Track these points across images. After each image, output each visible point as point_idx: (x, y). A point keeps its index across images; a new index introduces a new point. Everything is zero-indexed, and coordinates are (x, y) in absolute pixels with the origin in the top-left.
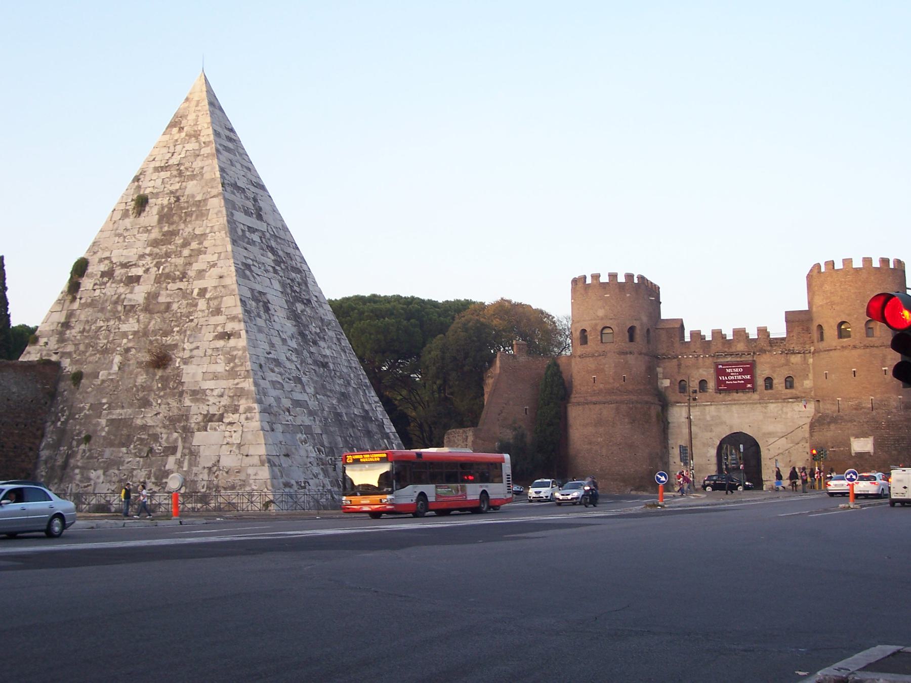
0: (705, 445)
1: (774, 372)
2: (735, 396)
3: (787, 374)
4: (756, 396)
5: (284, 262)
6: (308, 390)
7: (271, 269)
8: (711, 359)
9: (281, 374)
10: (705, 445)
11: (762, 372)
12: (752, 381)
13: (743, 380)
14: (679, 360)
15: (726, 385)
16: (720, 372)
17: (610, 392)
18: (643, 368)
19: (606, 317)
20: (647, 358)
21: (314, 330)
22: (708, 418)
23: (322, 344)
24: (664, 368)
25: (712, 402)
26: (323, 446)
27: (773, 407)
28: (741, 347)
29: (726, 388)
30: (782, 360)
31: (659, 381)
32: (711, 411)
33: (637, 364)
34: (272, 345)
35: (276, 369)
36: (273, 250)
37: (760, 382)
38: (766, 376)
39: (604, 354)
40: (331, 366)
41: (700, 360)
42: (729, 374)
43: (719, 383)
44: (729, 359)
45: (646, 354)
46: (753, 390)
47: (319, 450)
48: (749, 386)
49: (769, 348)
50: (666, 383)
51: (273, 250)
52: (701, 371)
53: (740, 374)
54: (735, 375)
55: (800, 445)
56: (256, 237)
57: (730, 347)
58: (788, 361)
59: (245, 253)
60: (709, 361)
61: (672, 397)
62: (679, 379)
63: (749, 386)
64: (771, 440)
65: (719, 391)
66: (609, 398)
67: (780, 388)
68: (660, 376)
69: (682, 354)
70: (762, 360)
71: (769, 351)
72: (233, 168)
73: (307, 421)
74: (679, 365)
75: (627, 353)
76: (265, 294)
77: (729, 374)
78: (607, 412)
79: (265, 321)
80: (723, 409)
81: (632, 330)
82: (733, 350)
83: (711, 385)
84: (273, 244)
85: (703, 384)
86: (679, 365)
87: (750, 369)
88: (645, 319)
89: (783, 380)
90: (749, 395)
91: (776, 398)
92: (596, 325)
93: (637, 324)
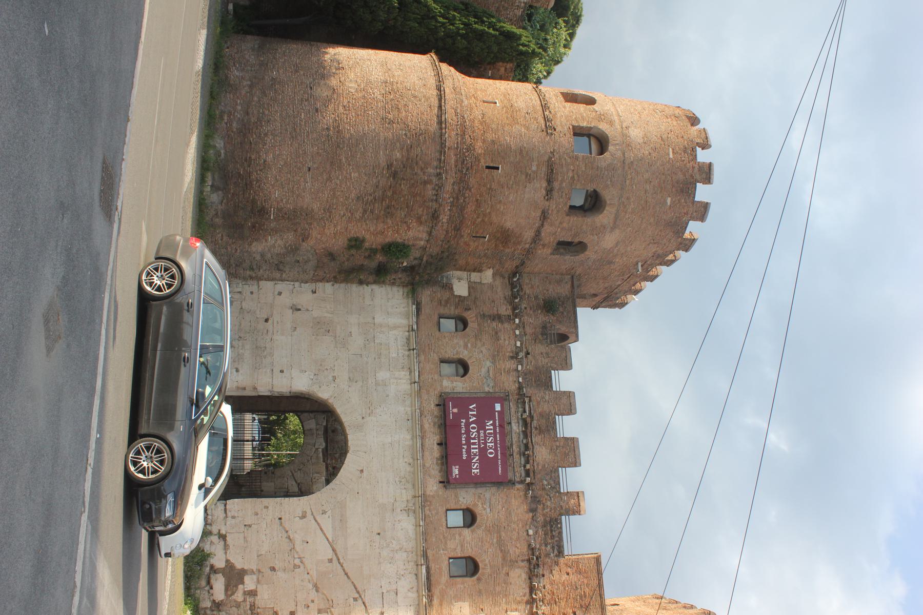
1: (488, 531)
2: (433, 439)
3: (484, 561)
4: (433, 486)
8: (514, 387)
11: (494, 505)
12: (467, 480)
13: (470, 458)
14: (510, 319)
15: (457, 417)
16: (485, 404)
18: (509, 224)
20: (529, 235)
22: (382, 375)
24: (491, 287)
25: (420, 386)
27: (405, 528)
28: (542, 454)
29: (448, 423)
30: (518, 549)
31: (464, 274)
32: (397, 383)
37: (466, 497)
38: (478, 510)
41: (511, 364)
42: (481, 426)
43: (462, 402)
44: (516, 428)
45: (538, 233)
46: (446, 482)
48: (456, 471)
49: (540, 519)
52: (488, 363)
53: (483, 451)
54: (479, 440)
55: (313, 594)
57: (540, 431)
58: (513, 563)
60: (509, 384)
61: (426, 295)
62: (470, 316)
63: (456, 471)
64: (327, 523)
65: (443, 403)
67: (451, 545)
68: (475, 277)
69: (522, 326)
70: (515, 503)
71: (533, 518)
74: (498, 318)
75: (549, 182)
77: (481, 426)
80: (403, 409)
82: (536, 439)
83: (459, 386)
86: (498, 318)
88: (609, 240)
89: (468, 552)
90: (436, 472)
91: (427, 534)
92: (611, 123)
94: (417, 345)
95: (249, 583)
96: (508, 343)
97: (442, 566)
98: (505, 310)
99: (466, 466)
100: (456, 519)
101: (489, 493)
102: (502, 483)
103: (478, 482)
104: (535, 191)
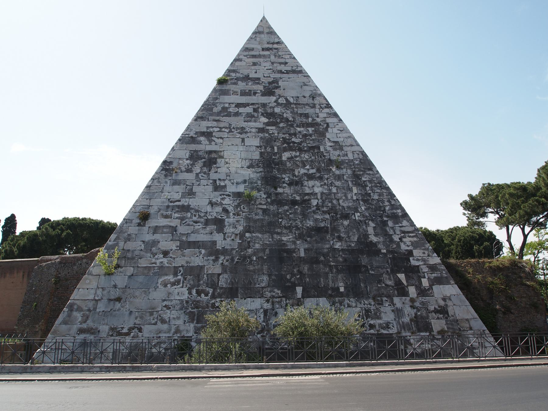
5: (287, 120)
6: (229, 230)
7: (254, 130)
9: (182, 219)
21: (302, 171)
23: (311, 183)
26: (214, 286)
34: (191, 193)
35: (177, 215)
36: (270, 115)
40: (314, 202)
47: (199, 293)
51: (270, 115)
56: (249, 110)
59: (215, 124)
72: (253, 67)
73: (197, 261)
76: (215, 152)
79: (197, 175)
84: (277, 110)
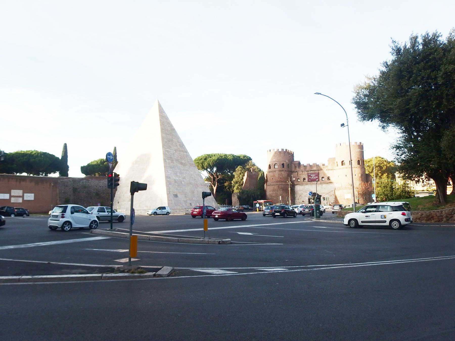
0: (305, 196)
10: (305, 196)
12: (318, 178)
16: (309, 176)
17: (277, 182)
19: (276, 161)
25: (307, 184)
27: (324, 185)
29: (311, 180)
32: (307, 187)
33: (284, 174)
37: (320, 178)
39: (275, 171)
43: (309, 179)
44: (312, 172)
50: (294, 179)
54: (313, 177)
60: (306, 173)
61: (295, 183)
65: (309, 181)
66: (276, 184)
78: (276, 187)
81: (283, 164)
82: (313, 169)
85: (304, 179)
87: (318, 175)
88: (287, 161)
93: (284, 163)
94: (302, 185)
95: (331, 203)
96: (301, 173)
97: (329, 181)
98: (297, 173)
99: (317, 178)
100: (323, 179)
101: (320, 175)
102: (319, 174)
103: (319, 177)
104: (283, 172)
